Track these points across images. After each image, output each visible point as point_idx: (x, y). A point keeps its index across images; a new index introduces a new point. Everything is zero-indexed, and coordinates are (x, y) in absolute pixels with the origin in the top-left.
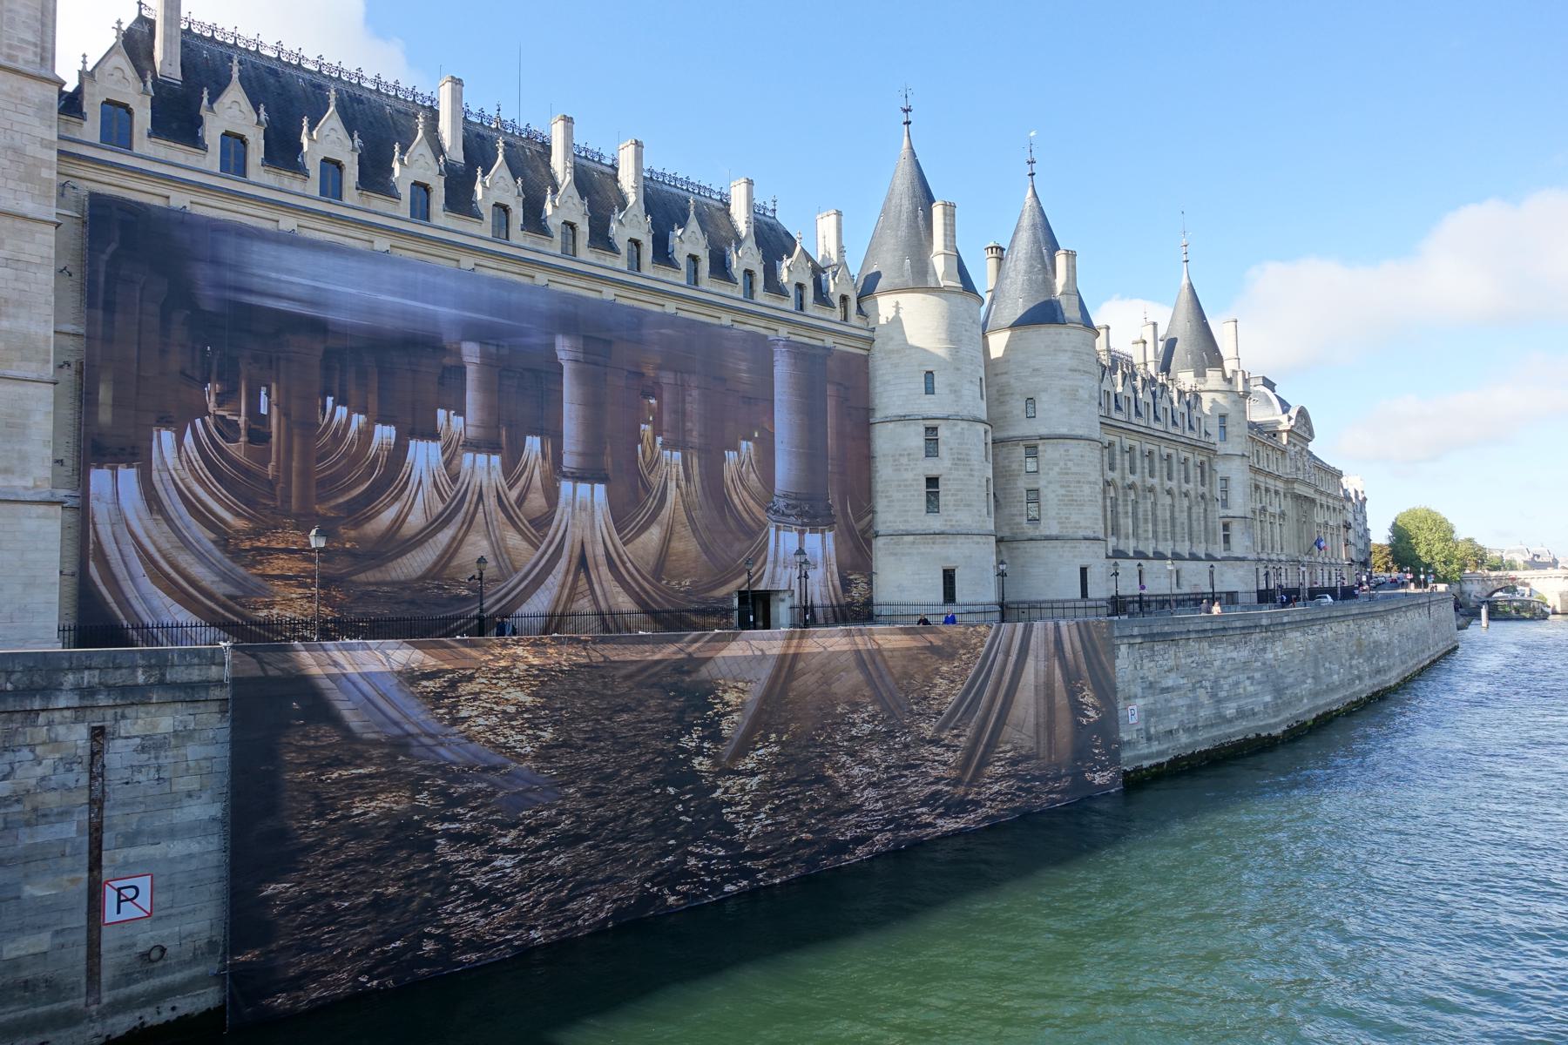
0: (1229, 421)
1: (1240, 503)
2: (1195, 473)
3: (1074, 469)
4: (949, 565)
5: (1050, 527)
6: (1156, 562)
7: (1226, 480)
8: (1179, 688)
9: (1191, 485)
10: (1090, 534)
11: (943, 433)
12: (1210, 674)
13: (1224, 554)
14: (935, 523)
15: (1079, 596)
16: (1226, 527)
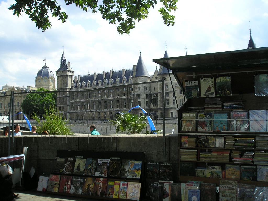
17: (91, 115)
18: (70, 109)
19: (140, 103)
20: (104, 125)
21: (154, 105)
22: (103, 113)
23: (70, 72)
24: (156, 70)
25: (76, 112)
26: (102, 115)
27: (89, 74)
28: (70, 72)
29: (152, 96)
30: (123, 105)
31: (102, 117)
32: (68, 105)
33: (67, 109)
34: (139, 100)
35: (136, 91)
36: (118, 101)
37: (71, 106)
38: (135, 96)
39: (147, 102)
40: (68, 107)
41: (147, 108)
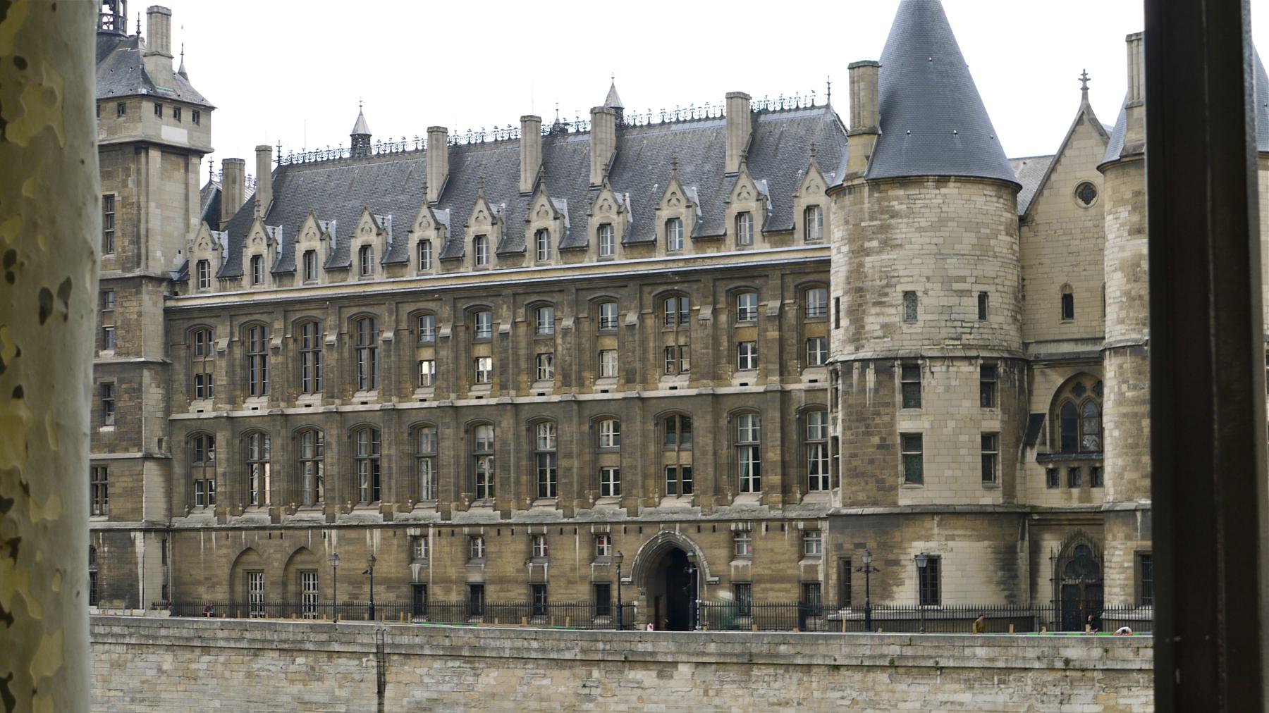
3: (1129, 394)
17: (389, 566)
18: (169, 493)
19: (920, 447)
20: (556, 673)
21: (1063, 474)
22: (520, 546)
23: (168, 111)
24: (1086, 117)
25: (232, 521)
26: (508, 559)
27: (360, 140)
28: (168, 111)
29: (1038, 378)
30: (733, 466)
31: (502, 581)
32: (148, 457)
33: (135, 492)
34: (906, 423)
35: (873, 323)
36: (675, 422)
37: (178, 470)
38: (871, 376)
39: (988, 440)
40: (152, 476)
41: (991, 498)
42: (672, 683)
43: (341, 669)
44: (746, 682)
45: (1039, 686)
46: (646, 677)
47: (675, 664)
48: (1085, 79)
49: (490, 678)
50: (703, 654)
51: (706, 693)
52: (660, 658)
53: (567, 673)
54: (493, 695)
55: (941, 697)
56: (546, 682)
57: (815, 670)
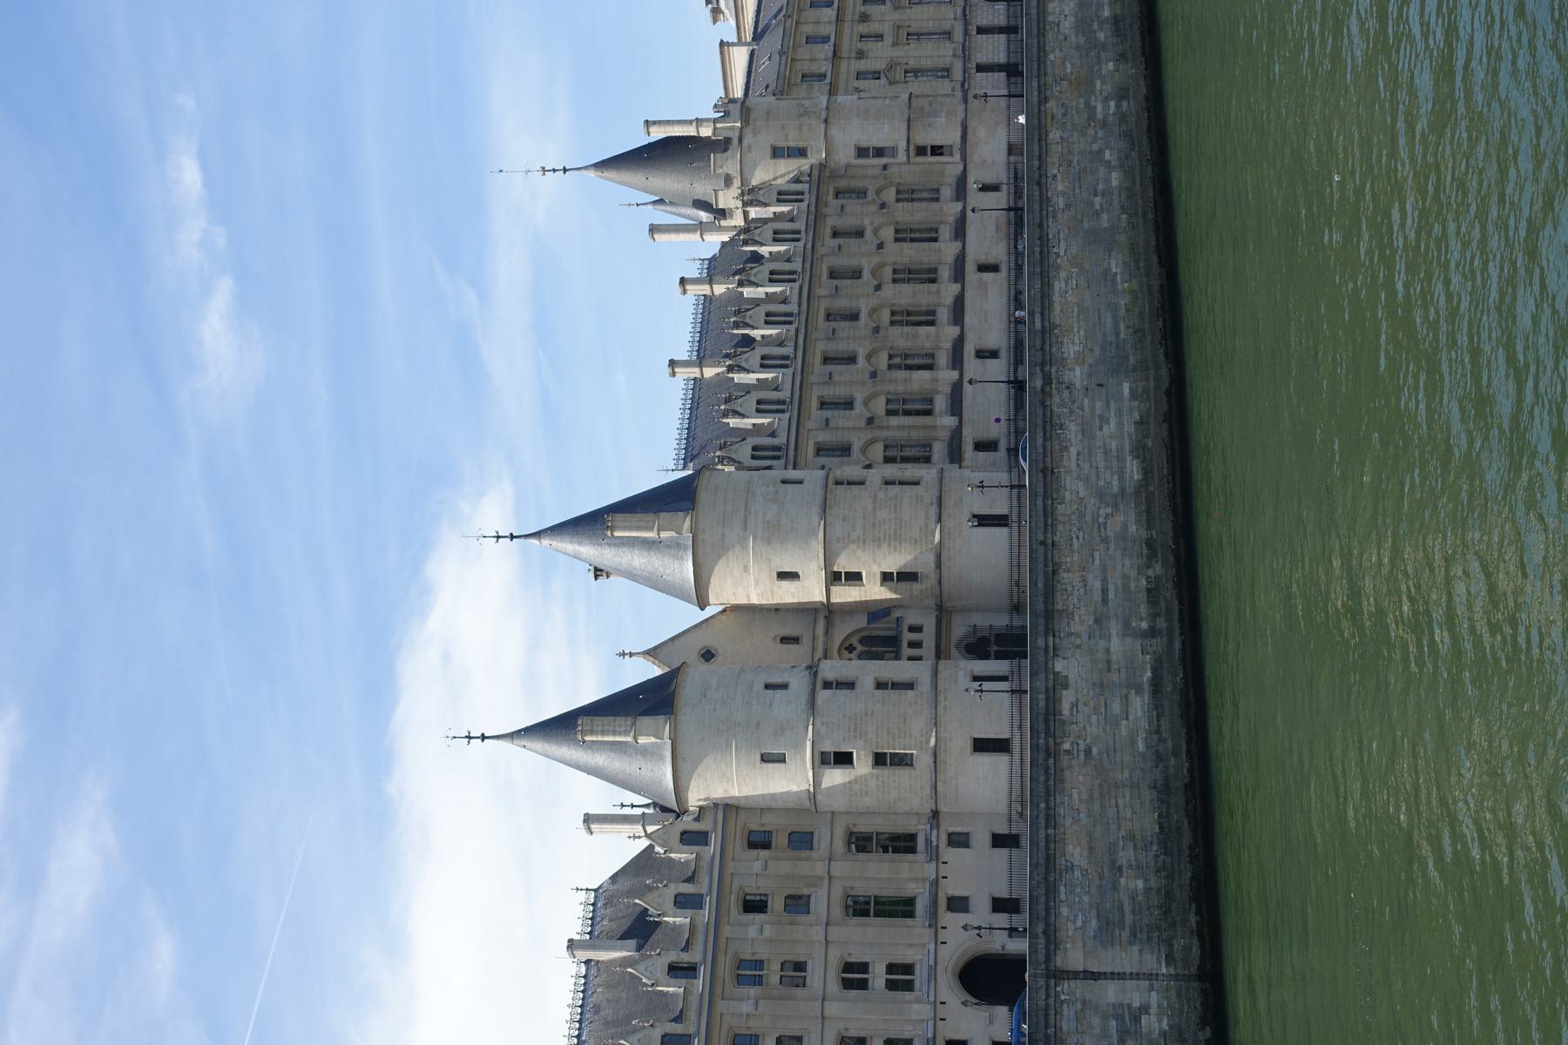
0: (781, 144)
1: (889, 133)
2: (858, 214)
4: (969, 745)
5: (926, 564)
6: (967, 320)
7: (862, 152)
8: (1104, 569)
9: (867, 222)
10: (934, 510)
11: (829, 747)
12: (1092, 502)
13: (957, 157)
14: (923, 761)
15: (1005, 530)
16: (921, 151)
20: (1068, 785)
42: (1071, 676)
43: (1073, 1025)
44: (1071, 616)
45: (1063, 405)
46: (1067, 698)
47: (1056, 674)
48: (623, 654)
49: (1075, 852)
50: (1046, 650)
51: (1078, 647)
52: (1051, 682)
53: (1067, 774)
54: (1091, 849)
55: (1074, 466)
56: (1075, 796)
57: (1056, 559)
